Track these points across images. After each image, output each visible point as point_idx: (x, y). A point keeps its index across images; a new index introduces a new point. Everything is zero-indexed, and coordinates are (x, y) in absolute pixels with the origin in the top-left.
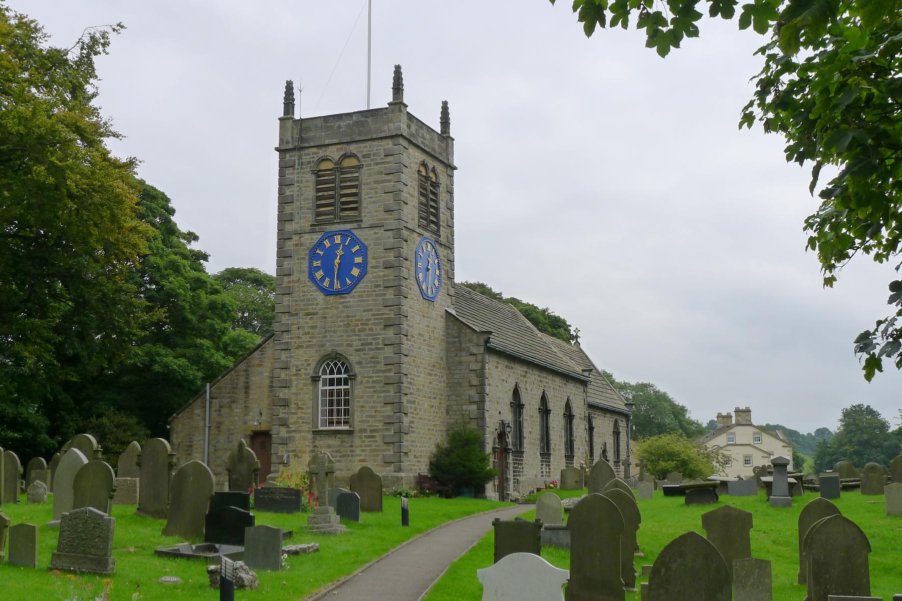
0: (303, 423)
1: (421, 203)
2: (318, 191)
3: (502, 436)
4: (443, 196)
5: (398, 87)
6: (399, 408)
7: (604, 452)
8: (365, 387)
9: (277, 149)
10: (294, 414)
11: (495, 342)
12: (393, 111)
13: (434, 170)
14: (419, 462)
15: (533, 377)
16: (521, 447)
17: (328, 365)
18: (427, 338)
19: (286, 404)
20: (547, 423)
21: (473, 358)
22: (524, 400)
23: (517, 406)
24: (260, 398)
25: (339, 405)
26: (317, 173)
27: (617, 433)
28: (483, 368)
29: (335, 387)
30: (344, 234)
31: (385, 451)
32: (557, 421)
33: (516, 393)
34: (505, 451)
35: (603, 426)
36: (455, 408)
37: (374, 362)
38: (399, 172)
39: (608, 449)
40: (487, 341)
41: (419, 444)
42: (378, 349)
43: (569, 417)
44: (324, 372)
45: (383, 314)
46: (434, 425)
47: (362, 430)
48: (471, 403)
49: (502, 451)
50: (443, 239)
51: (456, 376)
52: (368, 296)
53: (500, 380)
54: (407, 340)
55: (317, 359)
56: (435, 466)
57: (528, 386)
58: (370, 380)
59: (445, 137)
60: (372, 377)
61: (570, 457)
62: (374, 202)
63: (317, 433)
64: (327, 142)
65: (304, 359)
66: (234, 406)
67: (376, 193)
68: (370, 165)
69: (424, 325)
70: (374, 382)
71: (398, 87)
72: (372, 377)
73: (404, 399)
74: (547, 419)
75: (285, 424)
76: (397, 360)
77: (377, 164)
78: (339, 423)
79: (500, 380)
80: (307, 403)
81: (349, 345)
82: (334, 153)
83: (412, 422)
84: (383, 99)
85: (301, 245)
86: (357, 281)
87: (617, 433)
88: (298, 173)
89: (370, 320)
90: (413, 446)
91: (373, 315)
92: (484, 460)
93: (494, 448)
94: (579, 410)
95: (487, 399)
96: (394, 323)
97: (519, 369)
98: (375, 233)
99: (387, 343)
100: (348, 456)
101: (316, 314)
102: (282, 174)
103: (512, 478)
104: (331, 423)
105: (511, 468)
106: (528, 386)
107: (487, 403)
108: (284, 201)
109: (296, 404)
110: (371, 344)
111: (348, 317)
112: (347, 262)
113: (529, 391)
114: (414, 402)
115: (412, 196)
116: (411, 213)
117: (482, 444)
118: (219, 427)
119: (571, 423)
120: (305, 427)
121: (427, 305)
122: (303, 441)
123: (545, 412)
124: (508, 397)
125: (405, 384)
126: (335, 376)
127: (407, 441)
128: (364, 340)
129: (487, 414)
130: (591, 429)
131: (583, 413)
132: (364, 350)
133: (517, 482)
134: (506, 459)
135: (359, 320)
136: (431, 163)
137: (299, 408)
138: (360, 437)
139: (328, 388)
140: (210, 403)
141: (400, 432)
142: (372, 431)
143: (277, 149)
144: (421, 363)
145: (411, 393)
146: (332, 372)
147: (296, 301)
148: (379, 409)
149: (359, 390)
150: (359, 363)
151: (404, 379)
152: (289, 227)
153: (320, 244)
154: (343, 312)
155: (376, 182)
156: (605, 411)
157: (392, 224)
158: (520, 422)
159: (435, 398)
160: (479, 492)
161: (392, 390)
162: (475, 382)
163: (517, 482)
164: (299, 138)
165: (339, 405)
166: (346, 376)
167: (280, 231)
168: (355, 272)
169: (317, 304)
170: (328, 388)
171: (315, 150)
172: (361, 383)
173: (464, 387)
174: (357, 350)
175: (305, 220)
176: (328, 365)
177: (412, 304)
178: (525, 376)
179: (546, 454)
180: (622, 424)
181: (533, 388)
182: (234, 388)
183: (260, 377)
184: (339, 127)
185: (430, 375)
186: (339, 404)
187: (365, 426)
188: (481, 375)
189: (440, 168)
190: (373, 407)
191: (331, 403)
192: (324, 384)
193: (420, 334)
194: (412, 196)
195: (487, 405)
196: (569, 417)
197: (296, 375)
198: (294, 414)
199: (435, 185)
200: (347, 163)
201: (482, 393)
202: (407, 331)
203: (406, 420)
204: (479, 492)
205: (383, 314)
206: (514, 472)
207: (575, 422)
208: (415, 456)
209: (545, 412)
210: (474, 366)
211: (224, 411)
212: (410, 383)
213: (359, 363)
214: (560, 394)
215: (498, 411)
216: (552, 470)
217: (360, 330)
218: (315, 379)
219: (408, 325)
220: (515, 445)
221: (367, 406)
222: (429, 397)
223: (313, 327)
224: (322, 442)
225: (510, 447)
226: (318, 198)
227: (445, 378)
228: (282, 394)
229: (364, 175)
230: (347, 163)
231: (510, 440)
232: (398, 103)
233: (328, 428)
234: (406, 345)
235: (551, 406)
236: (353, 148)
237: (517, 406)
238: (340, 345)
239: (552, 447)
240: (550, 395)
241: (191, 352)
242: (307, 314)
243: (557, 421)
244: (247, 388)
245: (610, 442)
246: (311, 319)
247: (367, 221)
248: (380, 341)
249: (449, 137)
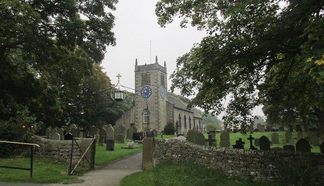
3: (177, 123)
4: (165, 79)
6: (159, 119)
11: (175, 106)
23: (180, 118)
24: (132, 117)
27: (200, 123)
30: (148, 87)
32: (187, 121)
35: (197, 122)
38: (157, 75)
43: (190, 120)
49: (177, 126)
53: (176, 113)
56: (165, 129)
59: (165, 68)
61: (190, 127)
65: (140, 110)
69: (163, 103)
75: (137, 122)
79: (176, 113)
80: (142, 119)
82: (145, 72)
84: (154, 62)
86: (150, 96)
92: (174, 128)
94: (192, 118)
96: (157, 103)
97: (180, 111)
108: (136, 81)
112: (148, 92)
116: (159, 83)
117: (174, 125)
122: (141, 125)
123: (185, 119)
124: (178, 116)
130: (194, 122)
136: (163, 73)
141: (159, 123)
152: (137, 86)
153: (143, 89)
156: (197, 118)
157: (156, 84)
160: (173, 134)
161: (157, 116)
164: (138, 69)
167: (135, 86)
168: (150, 94)
173: (170, 114)
175: (140, 84)
177: (160, 99)
179: (185, 127)
180: (201, 121)
183: (132, 114)
188: (173, 112)
196: (190, 120)
199: (164, 77)
204: (173, 134)
209: (185, 119)
215: (176, 119)
221: (152, 119)
229: (151, 76)
232: (157, 63)
236: (148, 71)
237: (180, 118)
241: (116, 109)
243: (187, 121)
244: (130, 116)
247: (152, 84)
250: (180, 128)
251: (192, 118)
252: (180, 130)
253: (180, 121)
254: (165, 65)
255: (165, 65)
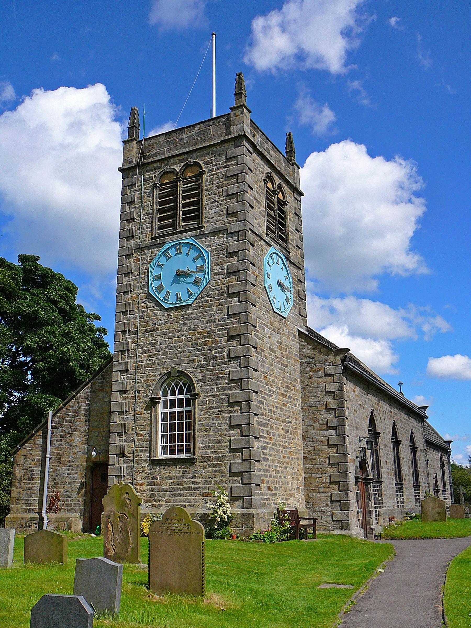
0: (141, 451)
2: (160, 204)
3: (362, 465)
6: (244, 429)
7: (436, 481)
8: (210, 408)
9: (120, 170)
10: (131, 441)
12: (235, 115)
13: (280, 187)
14: (274, 495)
15: (385, 407)
16: (379, 476)
17: (169, 385)
18: (279, 355)
20: (398, 454)
21: (330, 379)
22: (378, 430)
23: (374, 435)
25: (182, 429)
27: (442, 466)
28: (341, 389)
29: (177, 409)
31: (233, 482)
32: (405, 452)
33: (372, 422)
34: (367, 481)
36: (312, 433)
37: (219, 379)
39: (438, 480)
41: (273, 474)
42: (223, 363)
43: (414, 449)
44: (165, 394)
45: (228, 324)
46: (290, 453)
47: (206, 458)
48: (329, 428)
50: (292, 256)
51: (311, 400)
52: (211, 306)
54: (256, 352)
55: (157, 378)
57: (381, 415)
58: (215, 399)
60: (216, 396)
61: (417, 487)
62: (217, 206)
63: (155, 463)
64: (169, 155)
66: (75, 434)
67: (219, 197)
68: (212, 171)
70: (218, 401)
72: (216, 396)
73: (255, 420)
74: (398, 450)
76: (244, 375)
77: (219, 169)
78: (180, 451)
81: (191, 361)
83: (265, 448)
85: (143, 259)
87: (442, 466)
88: (140, 190)
89: (213, 331)
90: (266, 476)
91: (217, 326)
93: (356, 478)
94: (420, 443)
95: (347, 424)
98: (219, 238)
99: (232, 355)
100: (191, 488)
101: (156, 329)
102: (124, 193)
103: (374, 510)
104: (172, 452)
105: (373, 500)
106: (381, 415)
107: (347, 428)
109: (134, 430)
110: (215, 358)
111: (189, 330)
113: (383, 420)
114: (266, 425)
115: (258, 202)
116: (257, 218)
118: (59, 458)
119: (415, 455)
120: (144, 456)
121: (278, 320)
123: (396, 443)
124: (366, 425)
125: (255, 403)
126: (177, 397)
127: (259, 470)
128: (209, 354)
129: (348, 441)
131: (422, 446)
132: (207, 365)
133: (378, 514)
134: (367, 490)
135: (201, 333)
137: (138, 435)
138: (204, 467)
139: (169, 410)
140: (52, 432)
142: (217, 459)
143: (120, 170)
144: (274, 381)
145: (263, 414)
146: (173, 393)
147: (137, 318)
148: (226, 433)
149: (199, 410)
150: (202, 380)
151: (254, 396)
154: (185, 324)
155: (218, 187)
158: (377, 451)
159: (290, 422)
162: (332, 406)
163: (378, 514)
165: (182, 429)
166: (188, 396)
169: (157, 320)
170: (169, 410)
171: (157, 165)
172: (204, 403)
174: (200, 366)
176: (169, 385)
178: (378, 405)
179: (399, 485)
180: (445, 458)
181: (386, 416)
182: (75, 416)
184: (182, 139)
185: (283, 395)
186: (181, 429)
187: (209, 452)
189: (286, 189)
190: (218, 431)
191: (173, 429)
192: (165, 407)
193: (271, 349)
194: (258, 202)
195: (348, 430)
197: (134, 398)
198: (131, 441)
201: (341, 416)
202: (256, 343)
203: (256, 445)
205: (228, 324)
206: (375, 503)
207: (419, 453)
208: (269, 489)
209: (396, 443)
210: (331, 387)
211: (66, 440)
212: (261, 402)
213: (202, 380)
214: (407, 425)
216: (405, 500)
217: (203, 344)
219: (258, 337)
220: (374, 476)
222: (284, 421)
223: (152, 345)
224: (161, 471)
225: (371, 477)
226: (161, 211)
227: (300, 402)
231: (370, 469)
233: (168, 456)
234: (255, 358)
235: (400, 437)
237: (374, 435)
238: (182, 362)
239: (404, 477)
240: (399, 425)
242: (147, 331)
243: (405, 452)
245: (439, 473)
246: (151, 336)
247: (208, 227)
248: (225, 354)
249: (295, 163)
250: (379, 492)
251: (420, 443)
252: (378, 504)
253: (377, 456)
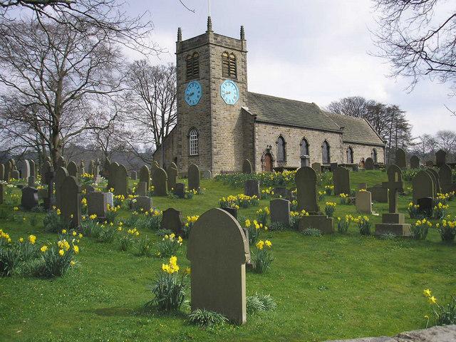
1: (222, 66)
2: (187, 67)
5: (209, 25)
19: (180, 146)
26: (187, 61)
40: (256, 118)
71: (209, 25)
82: (191, 53)
200: (196, 56)
218: (188, 137)
226: (188, 70)
228: (180, 143)
230: (196, 56)
236: (196, 50)
247: (201, 76)
254: (242, 34)
255: (242, 34)
